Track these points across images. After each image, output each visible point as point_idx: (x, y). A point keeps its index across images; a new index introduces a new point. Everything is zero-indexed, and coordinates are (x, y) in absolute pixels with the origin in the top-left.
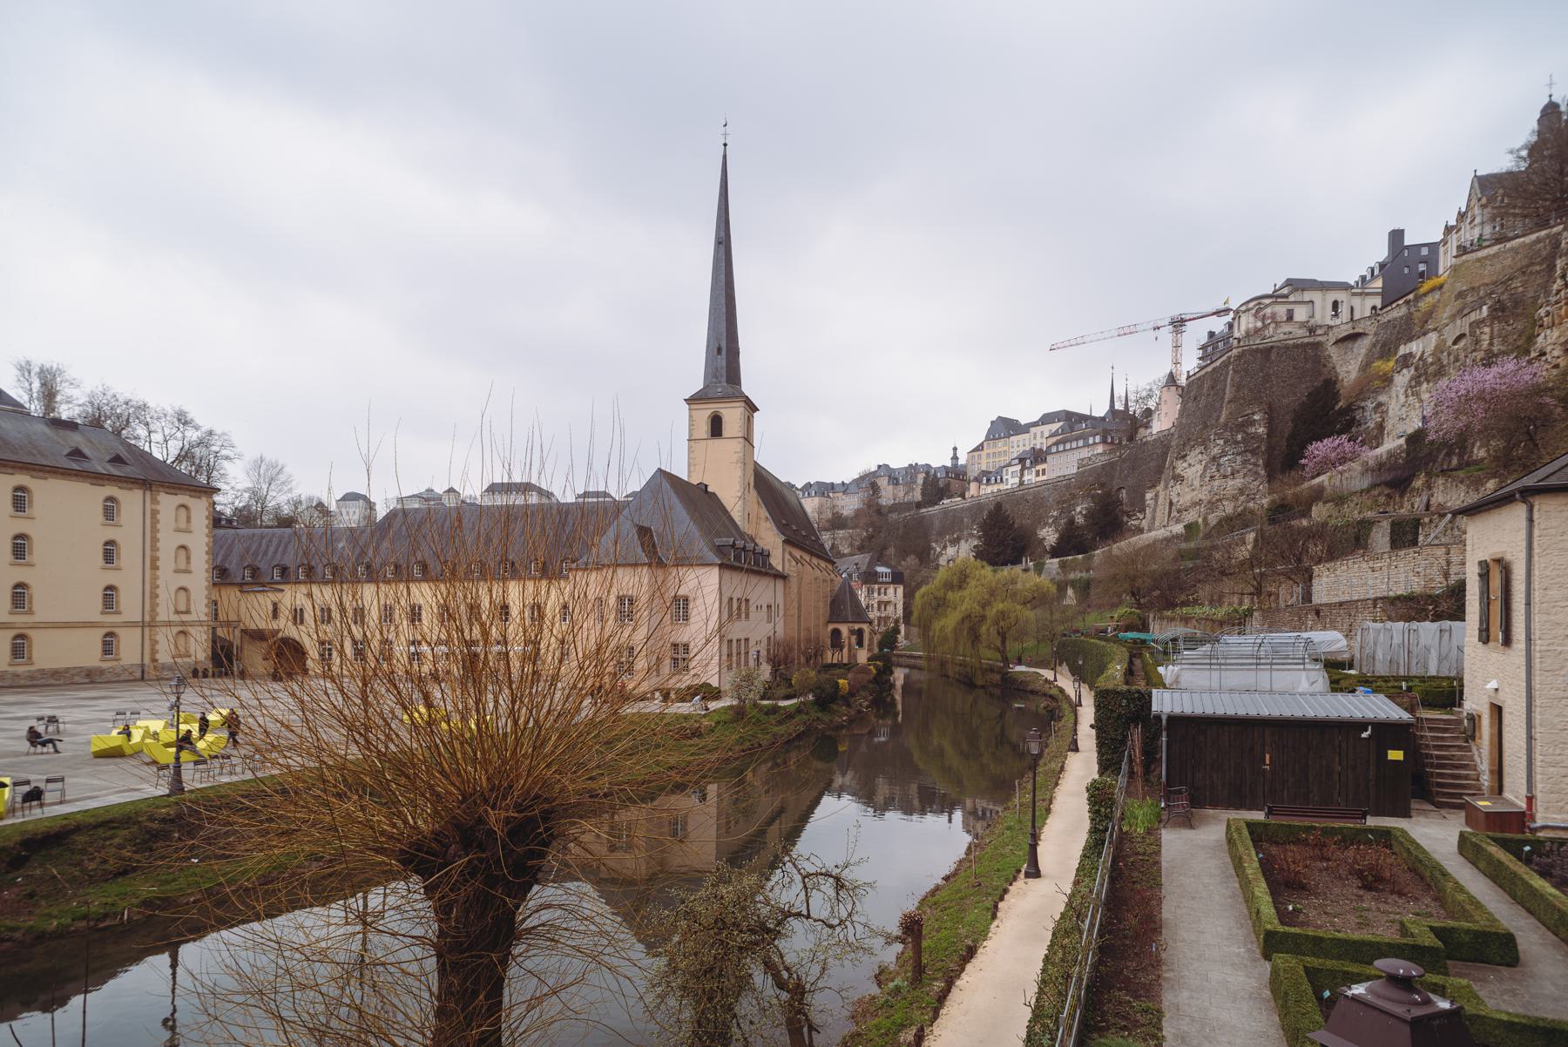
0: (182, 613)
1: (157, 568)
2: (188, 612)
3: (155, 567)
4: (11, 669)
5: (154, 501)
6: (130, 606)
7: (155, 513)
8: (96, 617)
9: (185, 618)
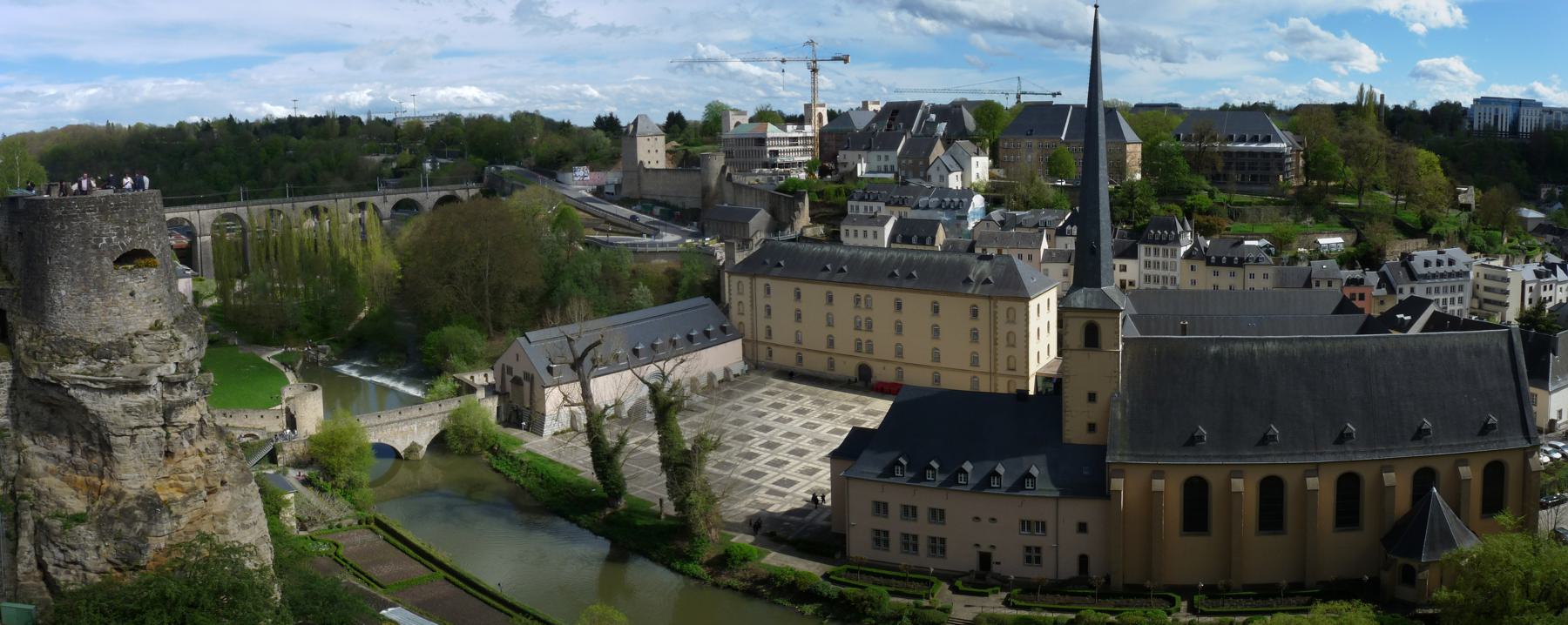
2: (1014, 370)
3: (996, 344)
5: (996, 307)
6: (984, 365)
7: (995, 313)
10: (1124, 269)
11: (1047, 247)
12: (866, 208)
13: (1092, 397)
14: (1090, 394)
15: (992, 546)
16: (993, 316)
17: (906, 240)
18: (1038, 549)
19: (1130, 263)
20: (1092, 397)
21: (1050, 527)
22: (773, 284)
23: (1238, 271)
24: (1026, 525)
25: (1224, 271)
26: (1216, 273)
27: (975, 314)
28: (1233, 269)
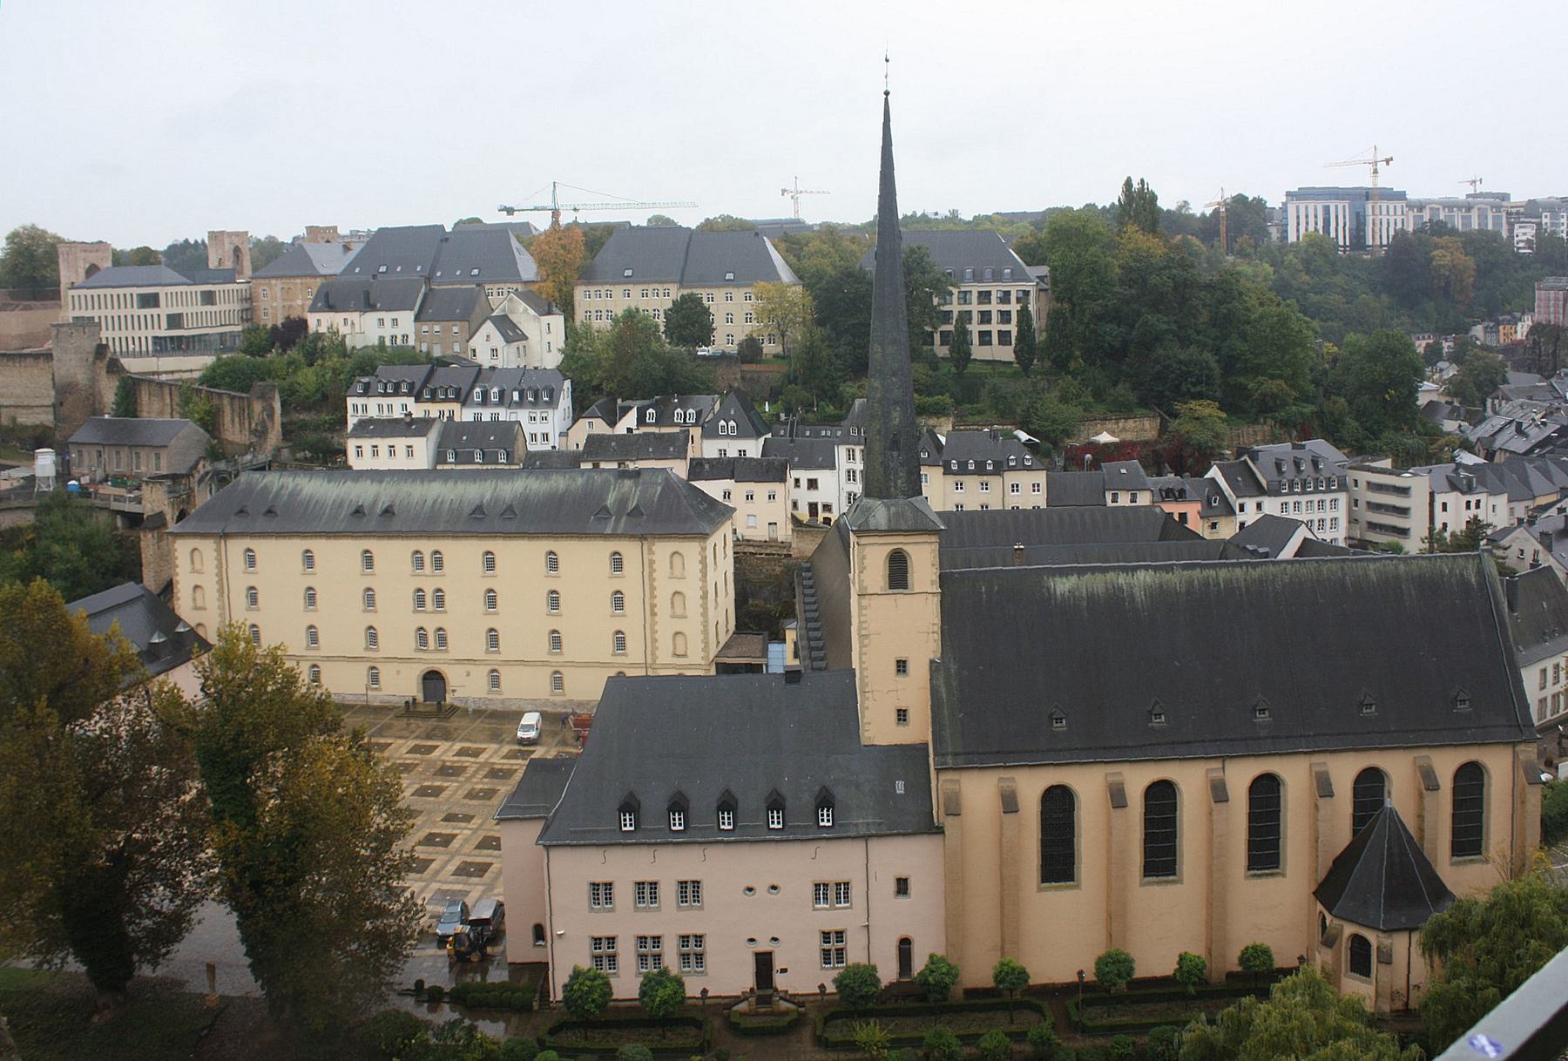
0: (679, 656)
1: (656, 614)
2: (685, 656)
3: (654, 614)
4: (551, 699)
5: (651, 552)
7: (652, 562)
8: (609, 659)
9: (681, 661)
10: (813, 484)
13: (901, 666)
14: (898, 662)
15: (775, 939)
16: (649, 569)
18: (840, 935)
19: (821, 475)
20: (901, 666)
21: (857, 891)
22: (261, 547)
23: (994, 482)
24: (820, 890)
25: (972, 482)
26: (959, 485)
28: (985, 478)
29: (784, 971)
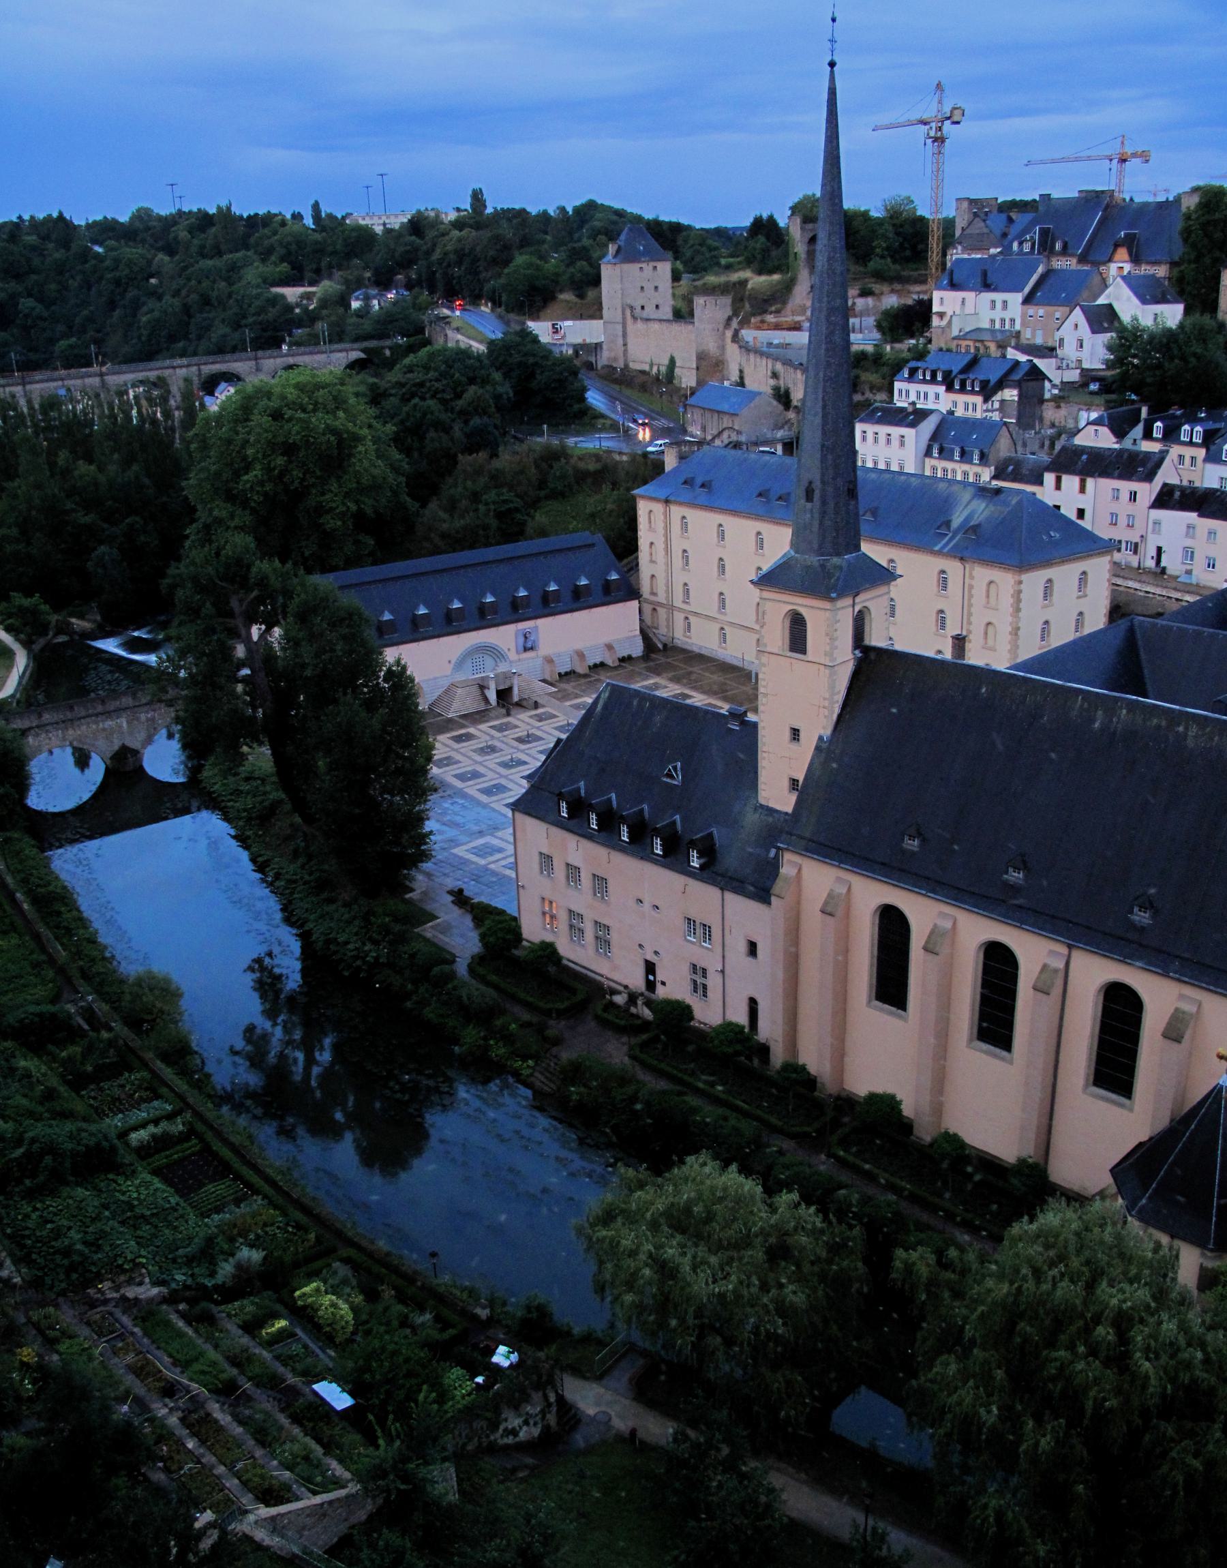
7: (971, 587)
11: (1174, 480)
12: (918, 393)
13: (795, 734)
17: (944, 454)
20: (795, 734)
27: (943, 583)
29: (663, 983)
